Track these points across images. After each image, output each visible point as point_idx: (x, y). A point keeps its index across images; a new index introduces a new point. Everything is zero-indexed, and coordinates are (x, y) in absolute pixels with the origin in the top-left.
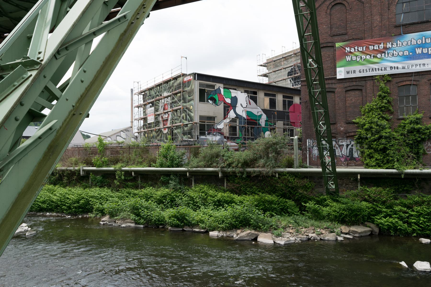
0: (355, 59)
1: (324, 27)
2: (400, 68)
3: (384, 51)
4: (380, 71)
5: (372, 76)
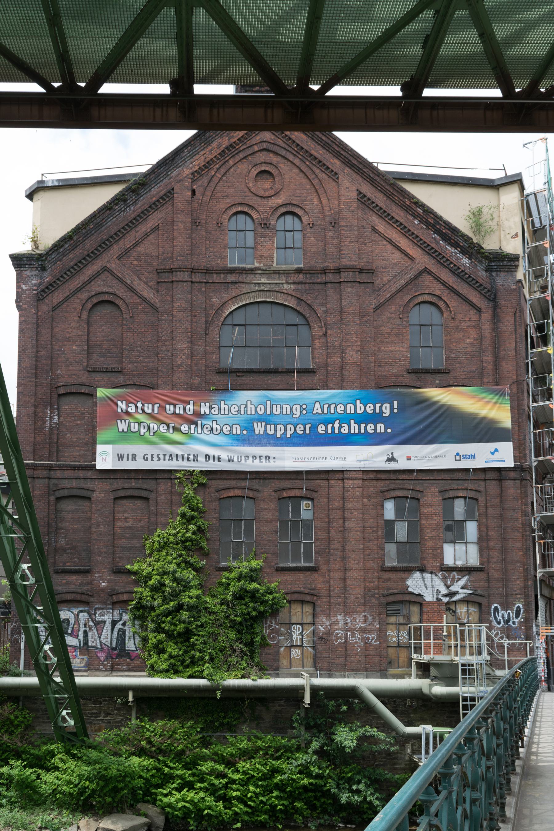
0: (136, 430)
1: (74, 347)
2: (224, 460)
3: (195, 419)
4: (185, 460)
5: (170, 471)
